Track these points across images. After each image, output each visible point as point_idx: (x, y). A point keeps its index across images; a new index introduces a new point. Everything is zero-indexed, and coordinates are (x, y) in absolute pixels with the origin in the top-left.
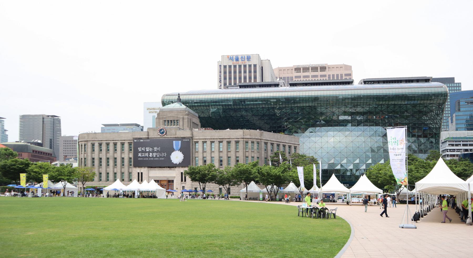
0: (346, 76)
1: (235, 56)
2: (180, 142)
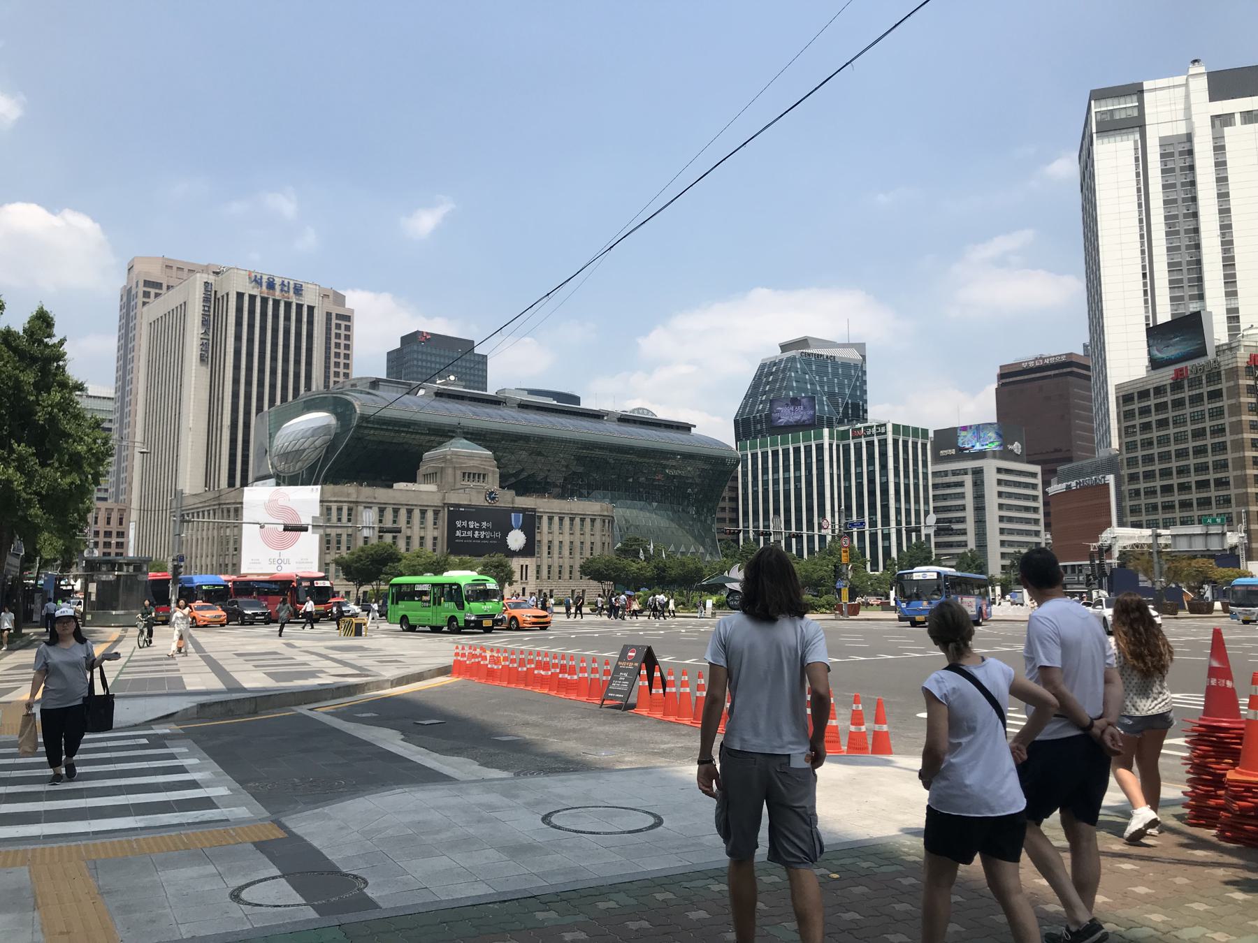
0: (340, 320)
1: (267, 277)
2: (521, 515)
